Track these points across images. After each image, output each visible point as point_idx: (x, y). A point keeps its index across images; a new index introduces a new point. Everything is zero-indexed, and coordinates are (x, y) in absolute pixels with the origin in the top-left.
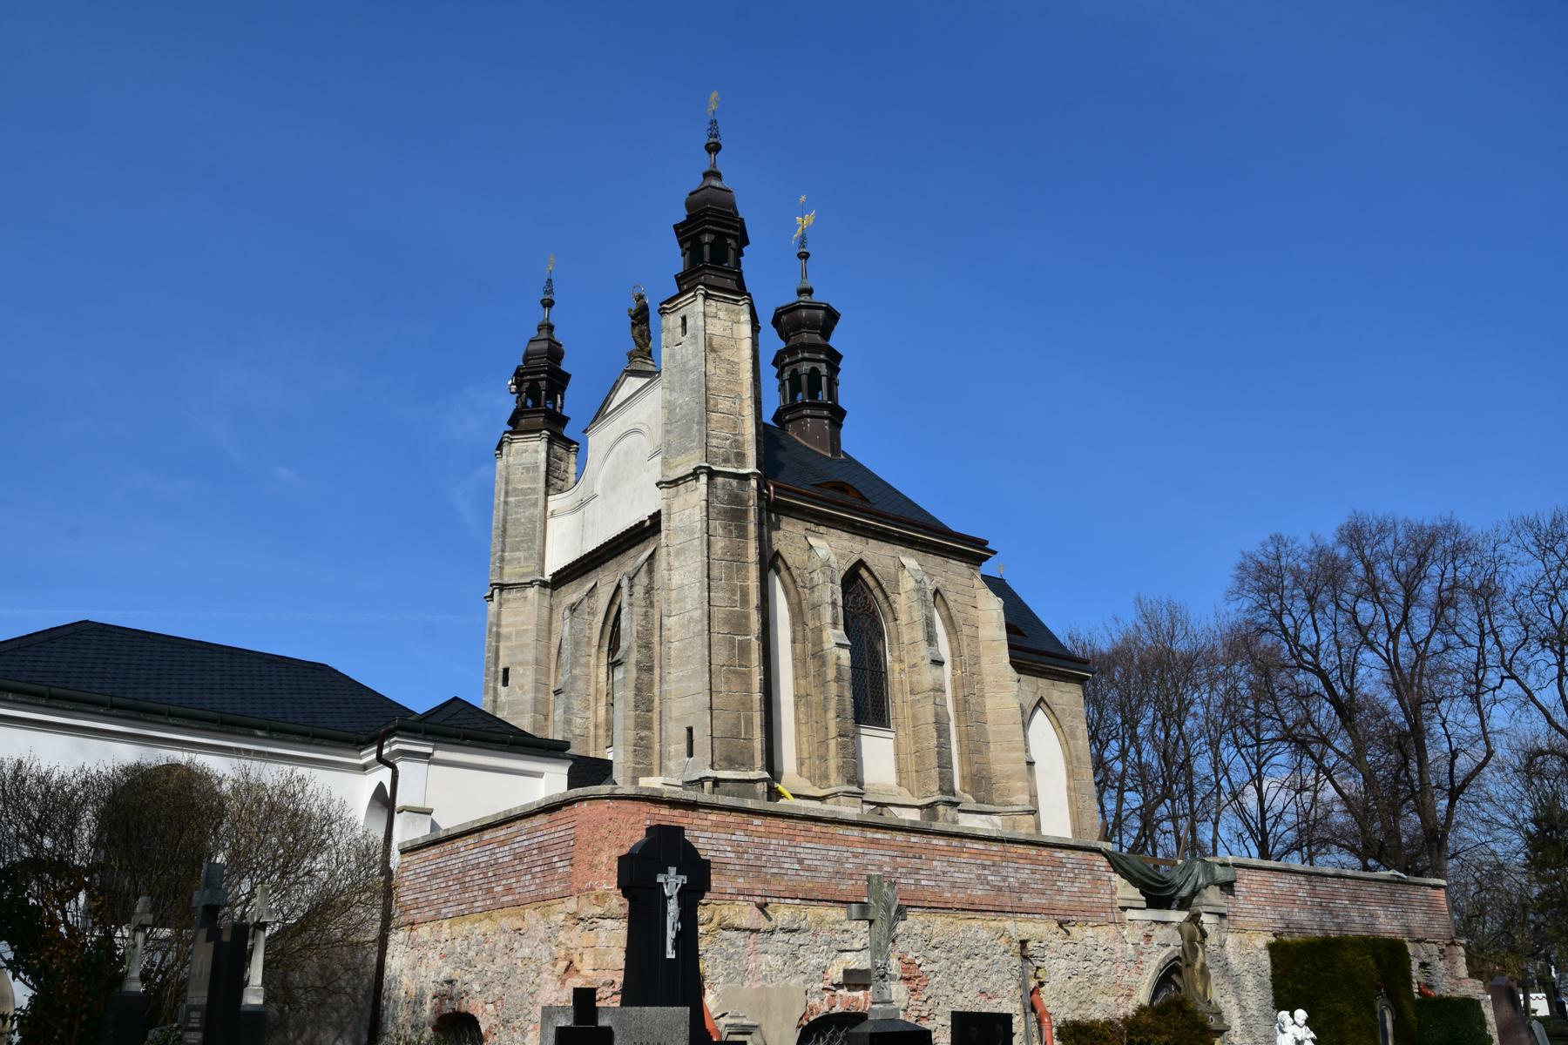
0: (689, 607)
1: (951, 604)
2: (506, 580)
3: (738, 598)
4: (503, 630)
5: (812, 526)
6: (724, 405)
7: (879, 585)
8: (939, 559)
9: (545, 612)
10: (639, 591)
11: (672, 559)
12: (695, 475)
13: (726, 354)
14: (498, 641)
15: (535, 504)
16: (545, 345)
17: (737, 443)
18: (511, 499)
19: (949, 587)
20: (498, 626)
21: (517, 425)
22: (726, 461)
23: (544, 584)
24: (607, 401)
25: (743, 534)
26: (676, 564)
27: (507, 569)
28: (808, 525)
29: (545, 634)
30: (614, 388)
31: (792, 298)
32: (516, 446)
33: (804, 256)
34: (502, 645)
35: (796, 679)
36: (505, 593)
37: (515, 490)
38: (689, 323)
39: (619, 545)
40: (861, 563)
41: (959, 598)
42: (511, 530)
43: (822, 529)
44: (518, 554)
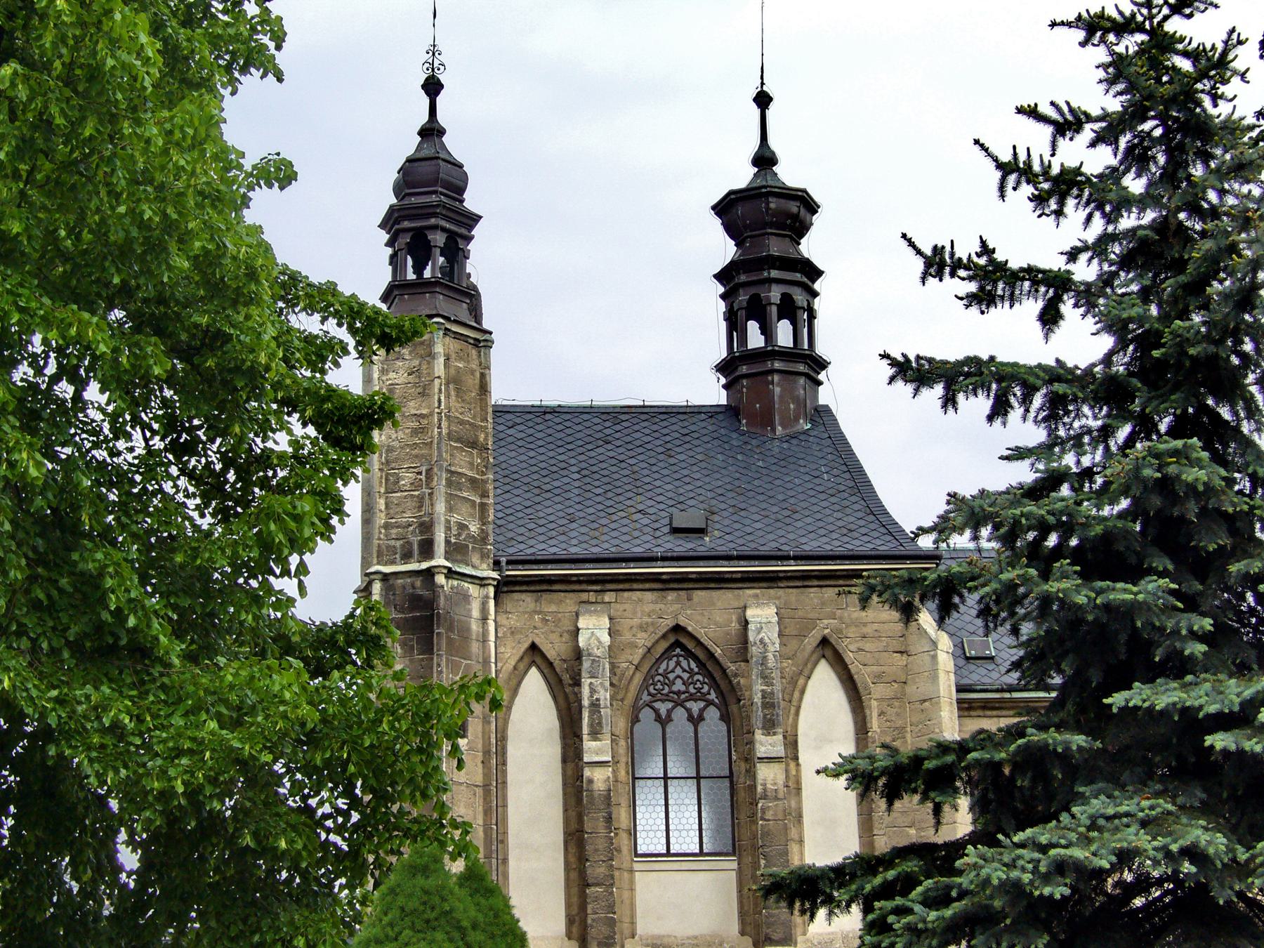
1: (849, 657)
5: (592, 597)
6: (407, 478)
7: (711, 655)
8: (830, 593)
17: (426, 527)
19: (852, 632)
22: (407, 557)
25: (428, 647)
28: (584, 596)
31: (742, 176)
33: (763, 100)
35: (565, 810)
40: (678, 629)
41: (868, 646)
43: (608, 597)
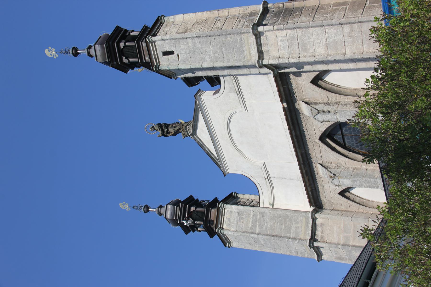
0: (341, 38)
2: (309, 237)
3: (341, 7)
4: (342, 241)
9: (335, 212)
10: (326, 108)
11: (308, 54)
12: (258, 36)
13: (190, 26)
14: (348, 245)
15: (263, 214)
16: (169, 207)
17: (244, 16)
18: (257, 231)
20: (338, 244)
21: (212, 229)
23: (315, 211)
24: (209, 154)
26: (312, 50)
27: (302, 237)
29: (348, 213)
30: (201, 145)
32: (225, 226)
34: (351, 243)
36: (318, 237)
37: (252, 228)
38: (167, 49)
39: (297, 136)
42: (277, 232)
44: (293, 228)
